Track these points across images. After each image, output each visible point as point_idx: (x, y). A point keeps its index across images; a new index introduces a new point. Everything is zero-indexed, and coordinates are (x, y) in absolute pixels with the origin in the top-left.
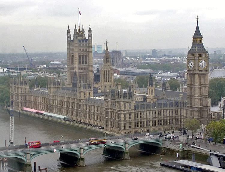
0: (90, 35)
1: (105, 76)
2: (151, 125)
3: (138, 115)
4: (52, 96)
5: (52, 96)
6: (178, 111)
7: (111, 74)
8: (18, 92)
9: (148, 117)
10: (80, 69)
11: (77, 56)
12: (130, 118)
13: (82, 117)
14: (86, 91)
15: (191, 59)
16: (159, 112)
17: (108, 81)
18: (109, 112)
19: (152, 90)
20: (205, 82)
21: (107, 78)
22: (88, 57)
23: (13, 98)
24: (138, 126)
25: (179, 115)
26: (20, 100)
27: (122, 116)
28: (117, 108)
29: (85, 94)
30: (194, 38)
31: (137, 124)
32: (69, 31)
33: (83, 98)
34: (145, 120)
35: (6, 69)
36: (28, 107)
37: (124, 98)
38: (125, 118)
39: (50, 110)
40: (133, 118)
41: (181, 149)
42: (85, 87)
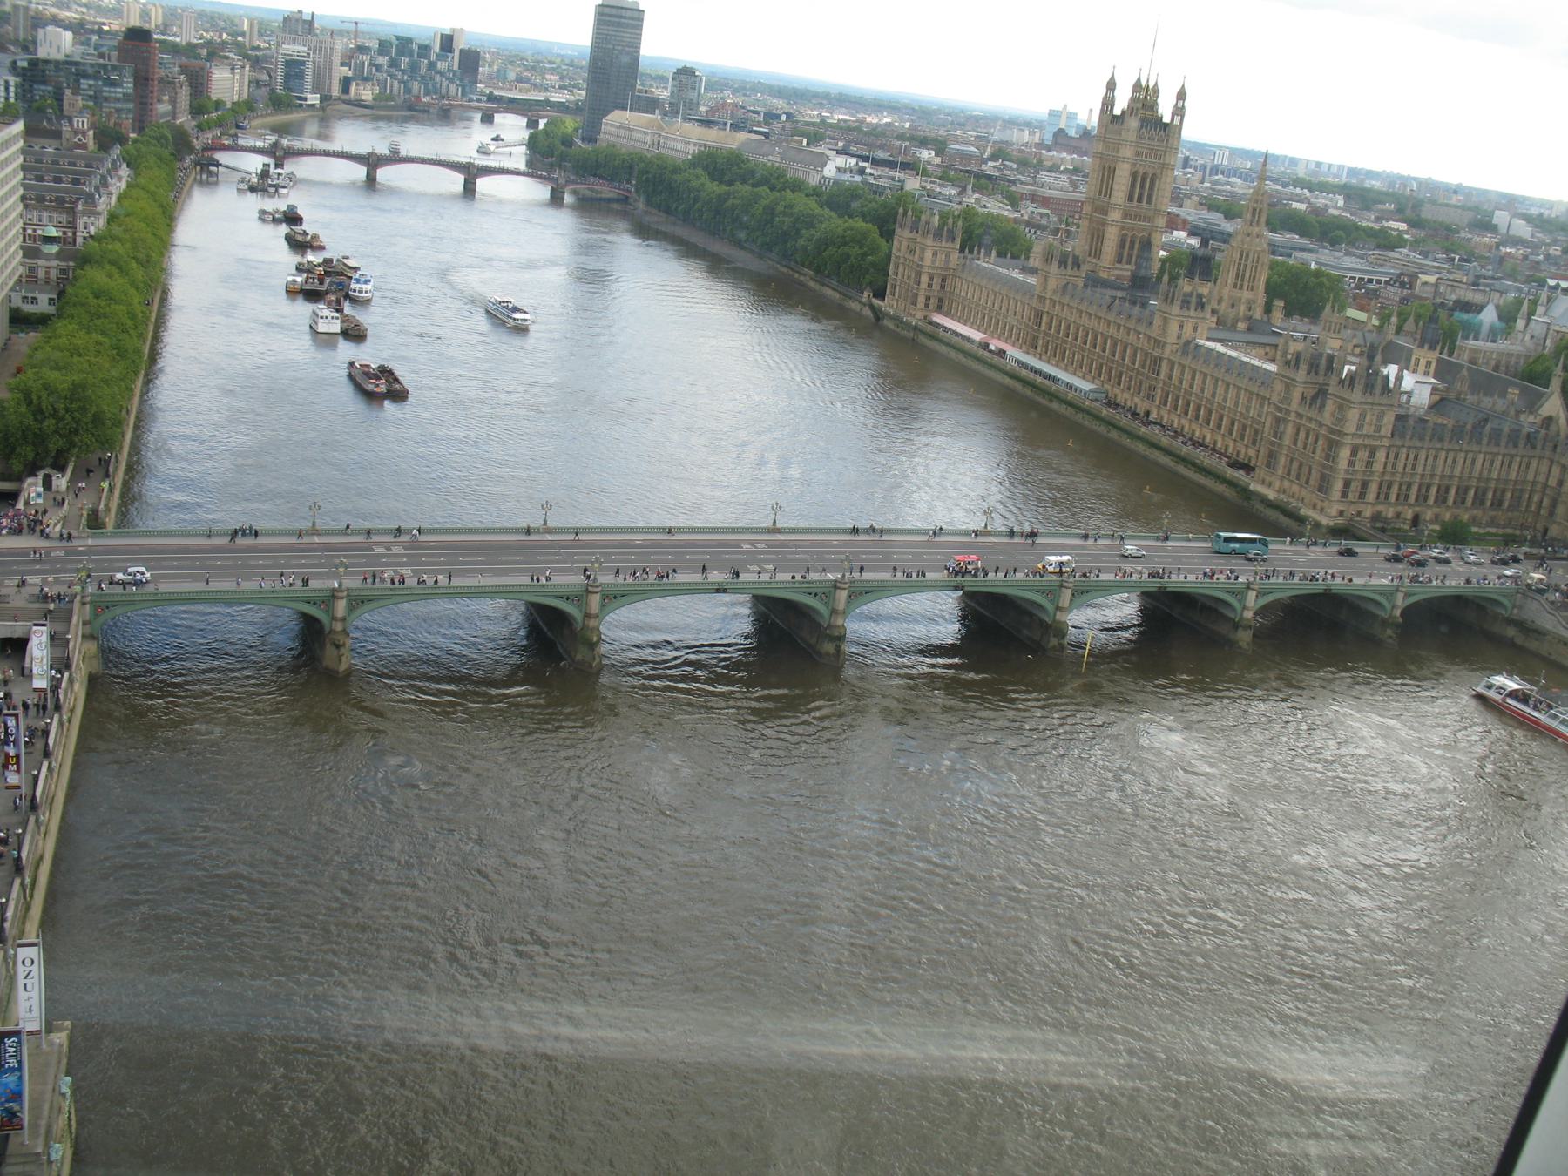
0: (1179, 111)
2: (1431, 500)
4: (1048, 302)
5: (1048, 302)
8: (922, 259)
9: (1429, 468)
10: (1126, 216)
12: (1369, 464)
16: (1469, 462)
19: (1428, 364)
21: (1243, 275)
23: (897, 275)
25: (1530, 477)
26: (924, 285)
27: (1345, 453)
29: (1181, 327)
31: (1384, 489)
32: (1111, 85)
33: (1171, 338)
34: (1418, 479)
35: (852, 161)
36: (948, 314)
37: (1364, 393)
38: (1351, 463)
39: (1032, 345)
40: (1378, 467)
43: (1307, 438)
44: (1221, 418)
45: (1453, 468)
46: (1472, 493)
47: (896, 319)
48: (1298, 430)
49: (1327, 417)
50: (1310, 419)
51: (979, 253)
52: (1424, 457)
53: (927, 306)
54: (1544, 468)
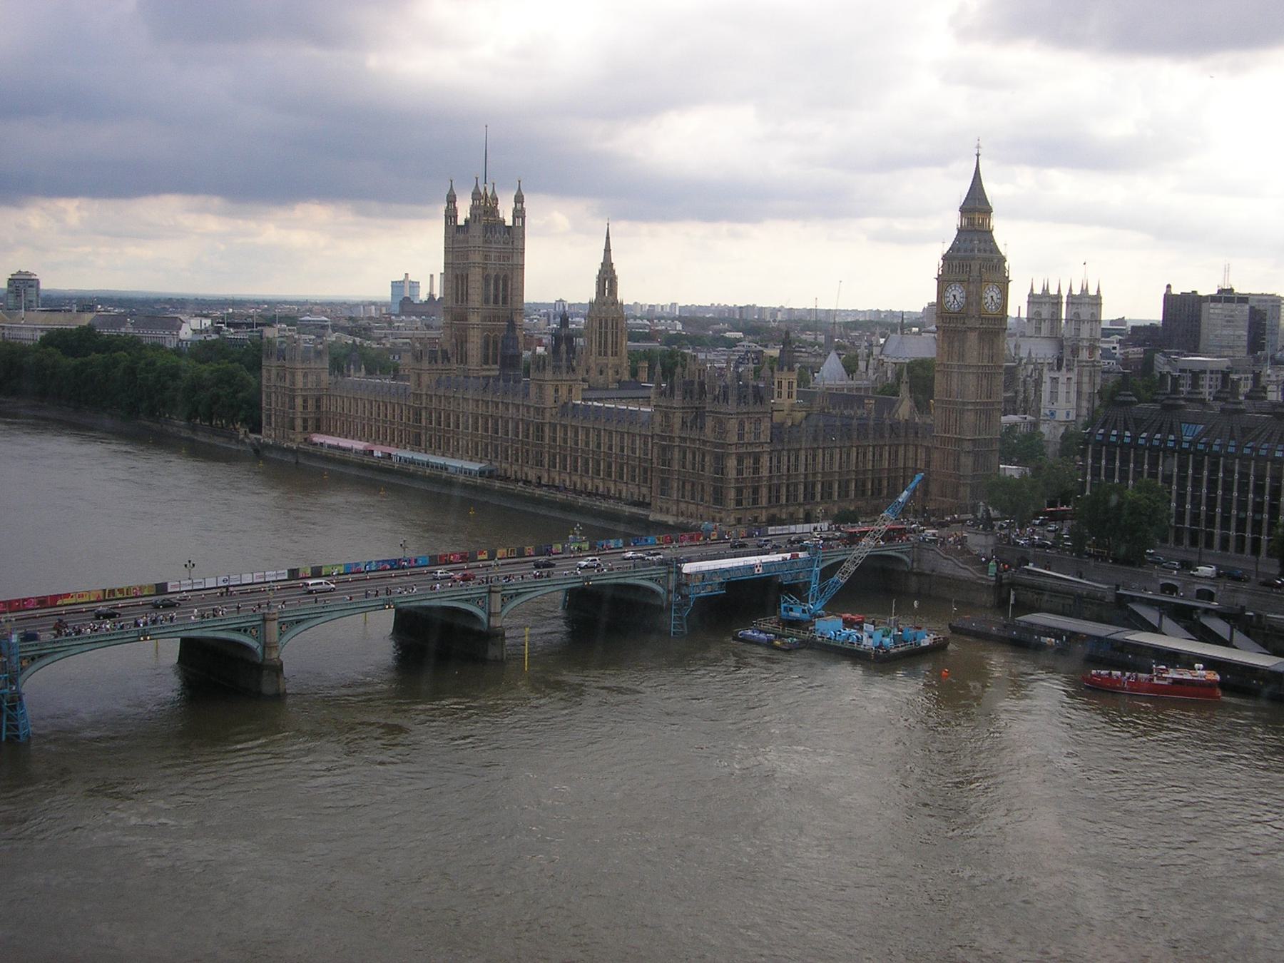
1: (600, 337)
2: (818, 498)
3: (779, 462)
4: (424, 397)
5: (424, 397)
6: (897, 452)
7: (619, 333)
8: (293, 383)
9: (810, 467)
10: (484, 319)
11: (479, 278)
12: (756, 470)
13: (547, 467)
14: (562, 380)
15: (956, 281)
17: (610, 353)
18: (676, 450)
19: (790, 384)
20: (995, 359)
22: (512, 280)
23: (271, 404)
24: (778, 498)
25: (901, 465)
27: (732, 463)
28: (709, 433)
29: (556, 391)
30: (964, 210)
31: (774, 493)
33: (549, 402)
36: (328, 433)
37: (738, 404)
38: (740, 472)
39: (416, 443)
40: (765, 472)
41: (994, 579)
42: (557, 368)
43: (694, 458)
44: (610, 467)
45: (831, 464)
46: (853, 485)
47: (276, 448)
48: (685, 454)
49: (709, 433)
50: (693, 441)
51: (349, 370)
52: (803, 457)
53: (305, 428)
54: (911, 454)
